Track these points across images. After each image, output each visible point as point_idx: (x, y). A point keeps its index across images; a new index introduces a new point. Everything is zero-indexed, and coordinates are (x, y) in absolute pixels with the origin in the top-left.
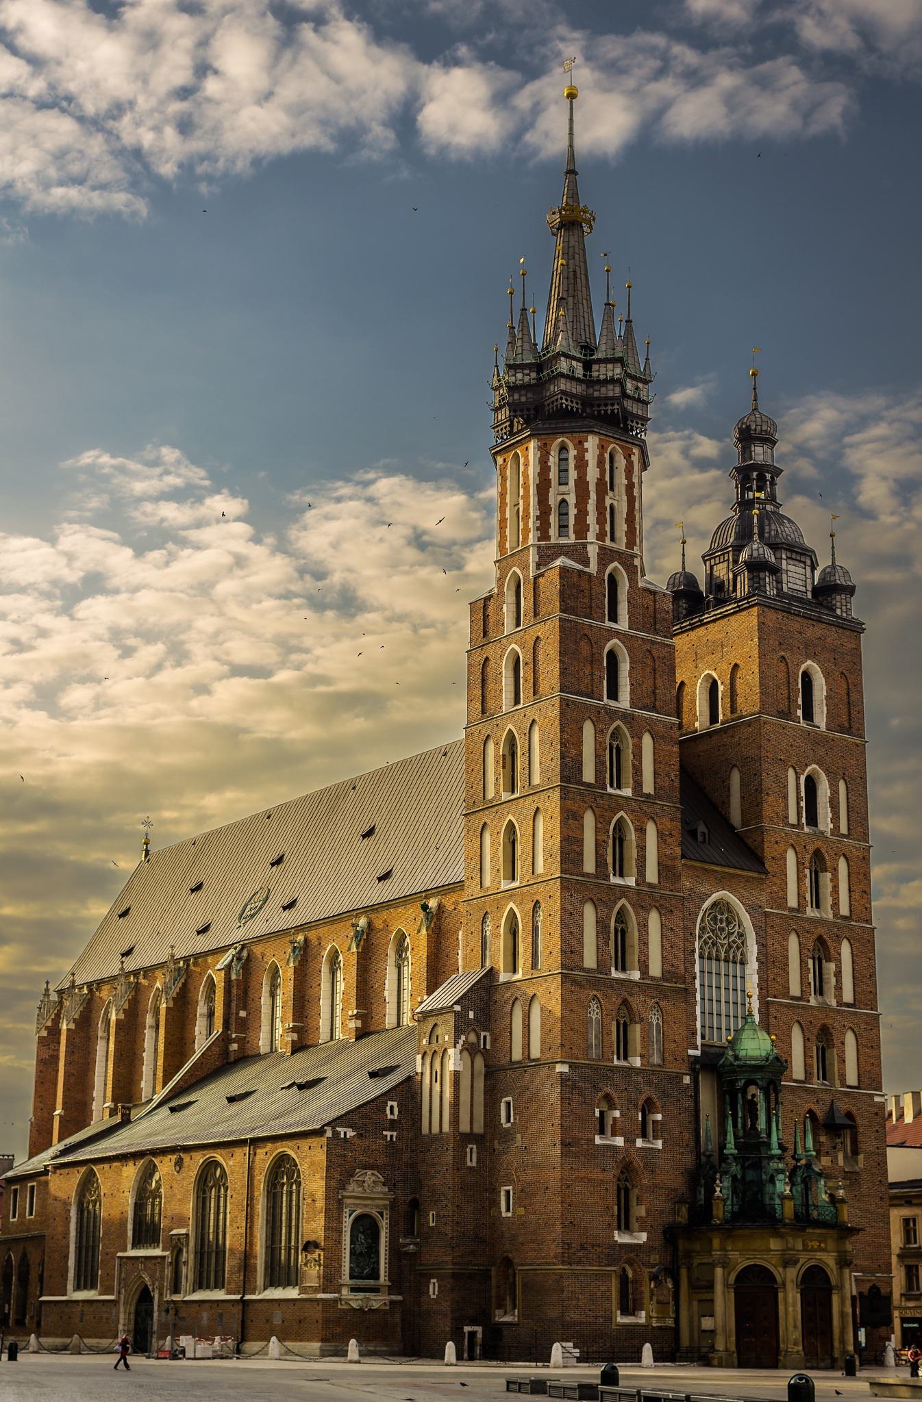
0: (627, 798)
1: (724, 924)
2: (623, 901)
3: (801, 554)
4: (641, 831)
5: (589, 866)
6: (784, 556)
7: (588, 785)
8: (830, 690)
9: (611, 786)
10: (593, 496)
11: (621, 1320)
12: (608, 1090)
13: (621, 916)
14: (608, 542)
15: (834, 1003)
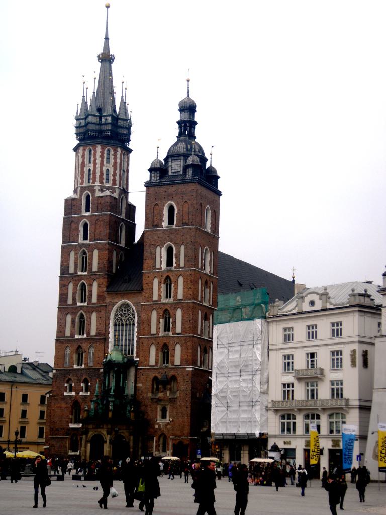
0: (85, 275)
1: (126, 312)
2: (82, 311)
3: (179, 156)
4: (91, 285)
5: (70, 301)
6: (170, 160)
7: (71, 274)
8: (179, 210)
9: (82, 271)
10: (80, 169)
11: (71, 453)
12: (70, 377)
13: (82, 316)
14: (85, 184)
15: (170, 334)
